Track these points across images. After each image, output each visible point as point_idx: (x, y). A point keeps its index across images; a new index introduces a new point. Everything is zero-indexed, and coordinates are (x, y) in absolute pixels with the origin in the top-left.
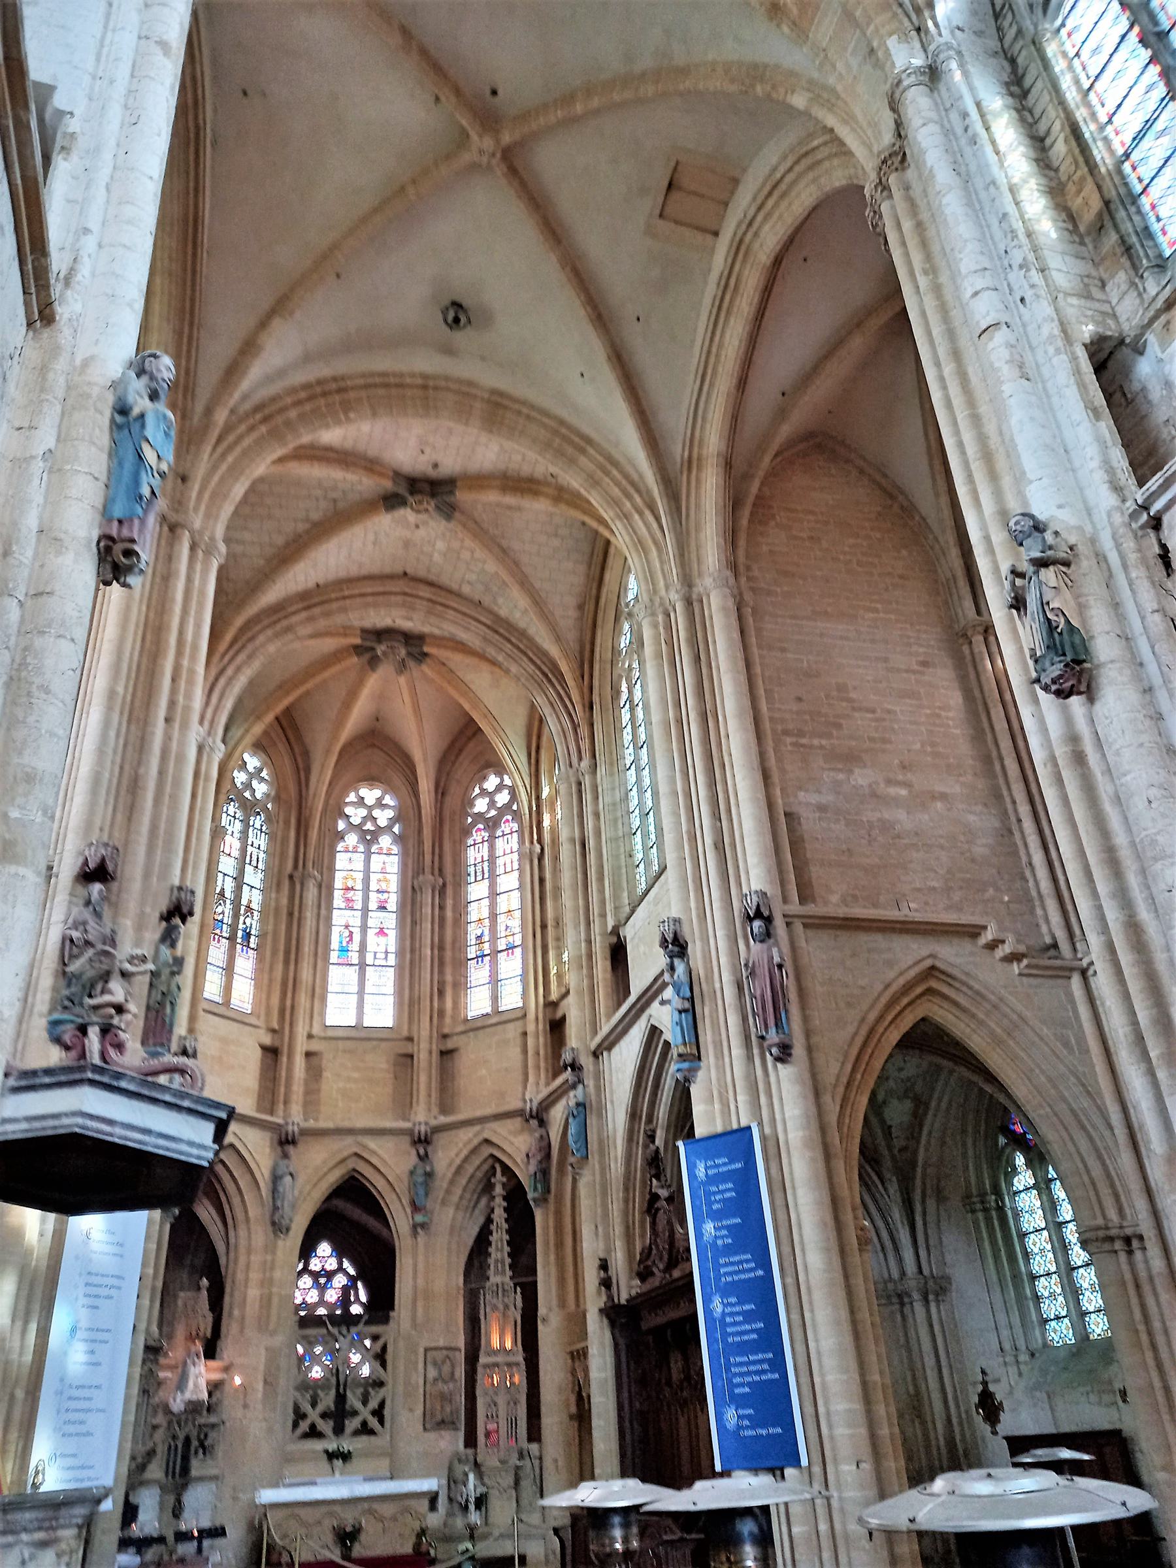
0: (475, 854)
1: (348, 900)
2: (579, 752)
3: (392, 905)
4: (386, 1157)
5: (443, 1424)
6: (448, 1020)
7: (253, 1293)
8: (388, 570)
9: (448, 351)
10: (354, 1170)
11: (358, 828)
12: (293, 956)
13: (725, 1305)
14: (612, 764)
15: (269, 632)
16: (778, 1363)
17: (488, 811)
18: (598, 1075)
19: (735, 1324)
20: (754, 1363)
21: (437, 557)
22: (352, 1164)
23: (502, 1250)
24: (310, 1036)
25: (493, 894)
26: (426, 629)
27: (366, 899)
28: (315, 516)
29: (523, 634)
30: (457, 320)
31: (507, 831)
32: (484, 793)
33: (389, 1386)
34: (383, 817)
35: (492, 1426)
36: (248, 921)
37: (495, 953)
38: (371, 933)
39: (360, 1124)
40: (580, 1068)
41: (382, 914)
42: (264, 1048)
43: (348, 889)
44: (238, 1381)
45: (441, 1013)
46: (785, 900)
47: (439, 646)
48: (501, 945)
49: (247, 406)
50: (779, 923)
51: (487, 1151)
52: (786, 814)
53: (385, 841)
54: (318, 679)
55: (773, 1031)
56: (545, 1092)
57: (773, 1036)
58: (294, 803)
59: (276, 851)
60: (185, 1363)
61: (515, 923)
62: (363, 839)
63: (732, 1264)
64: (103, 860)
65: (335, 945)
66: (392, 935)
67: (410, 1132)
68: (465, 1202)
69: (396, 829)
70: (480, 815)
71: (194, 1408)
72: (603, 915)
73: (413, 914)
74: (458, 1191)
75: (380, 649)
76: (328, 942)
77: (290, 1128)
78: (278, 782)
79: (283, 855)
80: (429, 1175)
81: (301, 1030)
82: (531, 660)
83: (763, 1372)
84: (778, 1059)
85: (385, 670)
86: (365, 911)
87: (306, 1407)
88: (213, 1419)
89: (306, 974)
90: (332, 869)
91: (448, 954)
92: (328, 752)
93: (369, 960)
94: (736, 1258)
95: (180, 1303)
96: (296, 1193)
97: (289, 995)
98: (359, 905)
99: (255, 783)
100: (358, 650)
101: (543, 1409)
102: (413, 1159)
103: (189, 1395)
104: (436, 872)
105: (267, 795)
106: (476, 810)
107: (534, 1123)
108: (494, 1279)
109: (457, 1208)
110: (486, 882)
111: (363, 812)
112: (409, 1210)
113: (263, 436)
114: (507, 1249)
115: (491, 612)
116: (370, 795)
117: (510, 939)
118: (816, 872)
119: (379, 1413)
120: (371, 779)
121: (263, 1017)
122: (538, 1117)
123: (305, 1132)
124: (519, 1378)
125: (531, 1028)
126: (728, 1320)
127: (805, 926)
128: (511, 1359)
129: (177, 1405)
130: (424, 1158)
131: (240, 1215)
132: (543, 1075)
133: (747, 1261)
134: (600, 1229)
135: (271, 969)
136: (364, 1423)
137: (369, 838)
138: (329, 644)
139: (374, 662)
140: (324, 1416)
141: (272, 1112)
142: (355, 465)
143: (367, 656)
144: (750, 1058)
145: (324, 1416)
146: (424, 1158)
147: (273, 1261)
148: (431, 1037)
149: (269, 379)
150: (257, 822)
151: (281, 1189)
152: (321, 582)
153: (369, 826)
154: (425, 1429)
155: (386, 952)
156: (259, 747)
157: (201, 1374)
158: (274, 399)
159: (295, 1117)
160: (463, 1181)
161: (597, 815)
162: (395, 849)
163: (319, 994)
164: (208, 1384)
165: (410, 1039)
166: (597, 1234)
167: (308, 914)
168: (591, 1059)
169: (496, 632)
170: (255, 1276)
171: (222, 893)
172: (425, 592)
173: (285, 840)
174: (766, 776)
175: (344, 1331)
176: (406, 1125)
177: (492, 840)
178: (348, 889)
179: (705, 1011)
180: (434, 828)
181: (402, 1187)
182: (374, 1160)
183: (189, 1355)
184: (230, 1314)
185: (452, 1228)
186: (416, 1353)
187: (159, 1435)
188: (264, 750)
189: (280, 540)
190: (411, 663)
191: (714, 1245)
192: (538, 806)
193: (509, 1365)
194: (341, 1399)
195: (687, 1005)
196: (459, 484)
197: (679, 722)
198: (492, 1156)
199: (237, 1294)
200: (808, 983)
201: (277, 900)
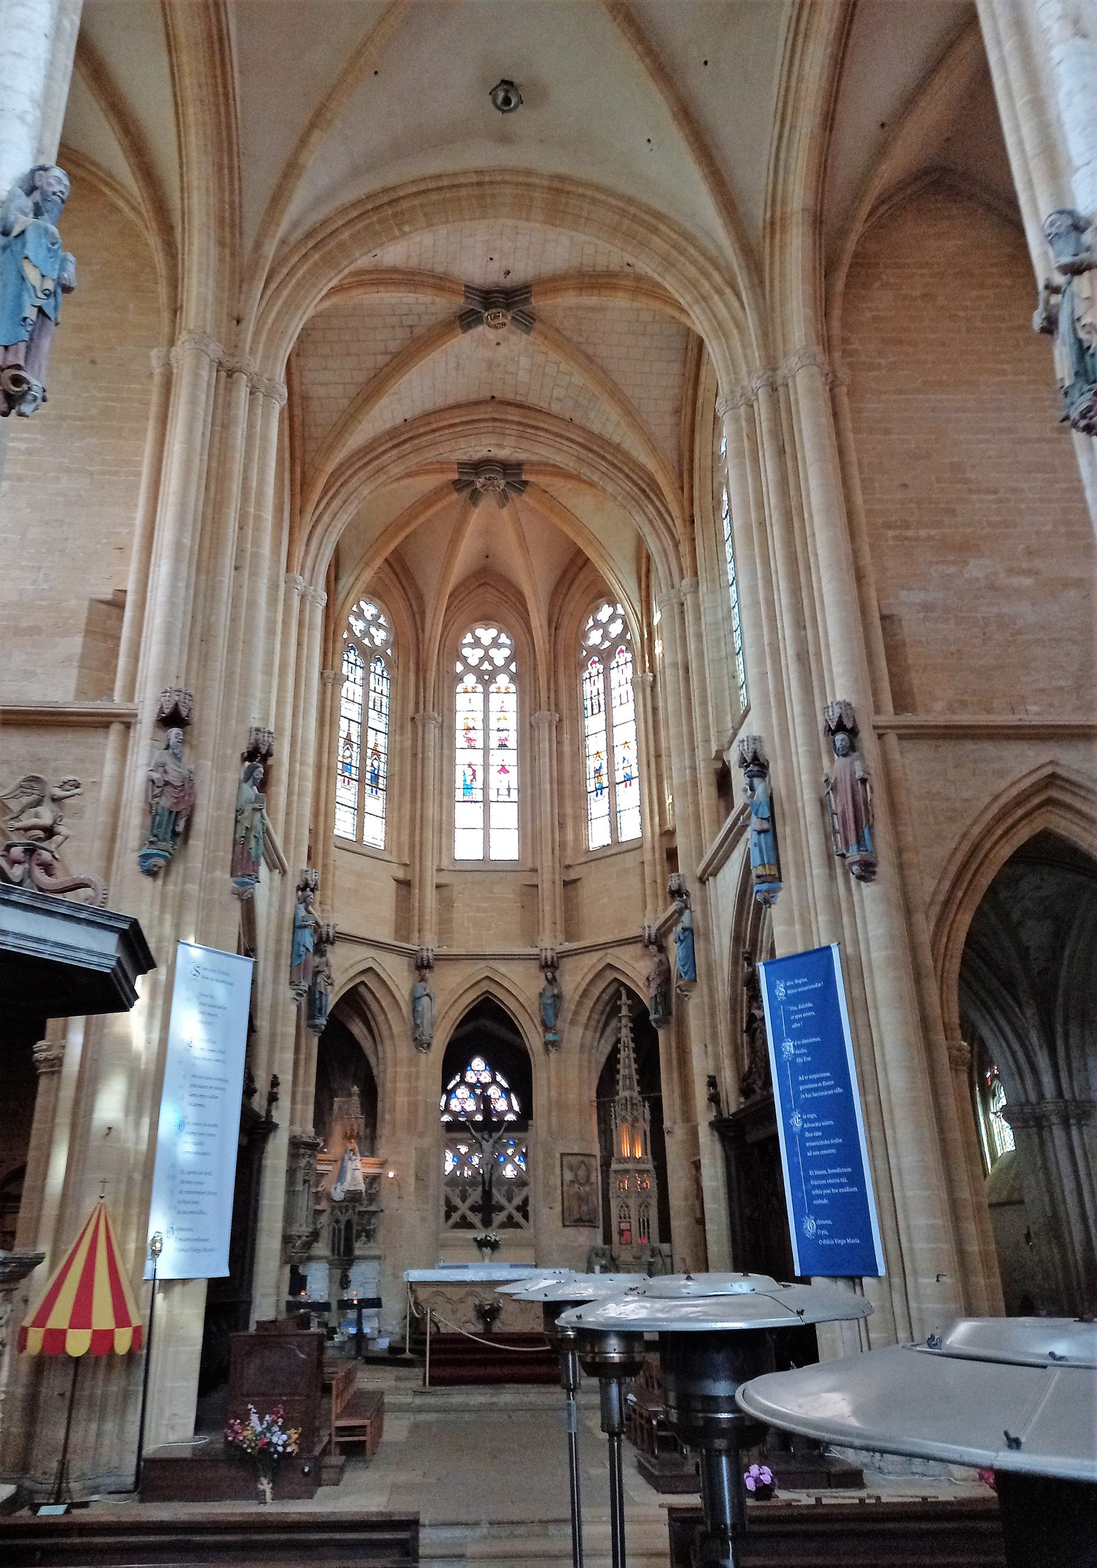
0: (592, 687)
1: (469, 740)
2: (681, 570)
3: (512, 743)
4: (516, 980)
5: (580, 1222)
6: (569, 852)
7: (401, 1100)
8: (473, 397)
9: (505, 139)
10: (487, 992)
11: (476, 670)
12: (419, 795)
13: (804, 1121)
14: (713, 581)
15: (362, 474)
16: (857, 1178)
17: (602, 643)
18: (704, 902)
19: (813, 1139)
20: (833, 1176)
21: (523, 376)
22: (485, 986)
23: (629, 1067)
24: (439, 870)
25: (609, 727)
26: (522, 456)
27: (486, 738)
28: (393, 346)
29: (617, 448)
30: (507, 101)
31: (622, 661)
32: (597, 625)
33: (531, 1186)
34: (500, 656)
35: (624, 1226)
36: (376, 763)
37: (613, 785)
38: (493, 771)
39: (489, 950)
40: (687, 894)
41: (503, 752)
42: (397, 881)
43: (469, 729)
45: (563, 845)
46: (878, 710)
47: (537, 473)
48: (619, 777)
49: (299, 234)
50: (867, 738)
51: (611, 975)
52: (883, 618)
53: (503, 680)
54: (422, 519)
55: (854, 848)
56: (662, 918)
57: (854, 855)
58: (412, 647)
59: (397, 696)
60: (343, 1160)
61: (631, 755)
62: (480, 679)
63: (813, 1081)
64: (176, 705)
65: (459, 783)
66: (514, 772)
67: (536, 958)
68: (593, 1023)
69: (513, 667)
70: (594, 650)
71: (353, 1197)
72: (707, 741)
73: (532, 749)
74: (585, 1013)
75: (479, 482)
76: (452, 781)
77: (425, 954)
78: (395, 629)
79: (404, 699)
80: (558, 997)
81: (430, 865)
82: (627, 476)
83: (842, 1185)
84: (860, 878)
85: (487, 503)
86: (486, 750)
87: (457, 1201)
88: (372, 1208)
89: (431, 810)
90: (452, 711)
91: (568, 787)
92: (440, 593)
93: (493, 796)
94: (816, 1076)
95: (336, 1107)
96: (435, 1012)
97: (418, 831)
98: (480, 744)
99: (373, 630)
100: (458, 485)
101: (672, 1213)
102: (543, 983)
103: (347, 1186)
104: (553, 706)
105: (385, 642)
106: (590, 643)
107: (653, 949)
108: (624, 1094)
109: (586, 1027)
110: (603, 714)
111: (480, 653)
112: (540, 1029)
113: (316, 264)
114: (634, 1066)
115: (582, 428)
116: (486, 635)
117: (628, 770)
118: (917, 680)
119: (523, 1209)
120: (486, 620)
121: (395, 853)
122: (657, 943)
123: (438, 958)
124: (650, 1183)
125: (648, 856)
126: (807, 1135)
127: (900, 737)
128: (642, 1166)
129: (338, 1195)
130: (552, 981)
131: (385, 1033)
132: (660, 903)
133: (827, 1079)
134: (710, 1049)
135: (400, 808)
136: (510, 1217)
137: (486, 679)
138: (428, 483)
139: (475, 497)
140: (473, 1209)
141: (407, 939)
142: (423, 284)
143: (466, 493)
144: (832, 877)
145: (473, 1209)
146: (552, 981)
147: (417, 1073)
148: (554, 868)
149: (317, 202)
150: (379, 668)
151: (420, 1009)
152: (408, 416)
153: (486, 666)
154: (564, 1226)
155: (509, 789)
156: (374, 594)
158: (324, 223)
159: (430, 944)
160: (590, 1003)
161: (699, 636)
162: (513, 688)
163: (446, 829)
164: (366, 1177)
165: (534, 870)
166: (706, 1053)
167: (431, 755)
168: (698, 885)
169: (590, 450)
170: (402, 1085)
171: (348, 739)
172: (514, 415)
173: (405, 684)
174: (860, 577)
175: (486, 1136)
176: (536, 951)
177: (606, 673)
178: (469, 729)
179: (785, 831)
180: (548, 664)
181: (533, 1007)
182: (505, 984)
183: (345, 1152)
184: (384, 1120)
185: (582, 1046)
186: (553, 1157)
187: (324, 1219)
188: (380, 597)
189: (361, 377)
190: (512, 494)
191: (793, 1062)
192: (650, 634)
193: (641, 1172)
194: (487, 1195)
195: (766, 825)
196: (534, 289)
197: (762, 524)
198: (616, 979)
199: (387, 1100)
200: (901, 797)
201: (402, 742)
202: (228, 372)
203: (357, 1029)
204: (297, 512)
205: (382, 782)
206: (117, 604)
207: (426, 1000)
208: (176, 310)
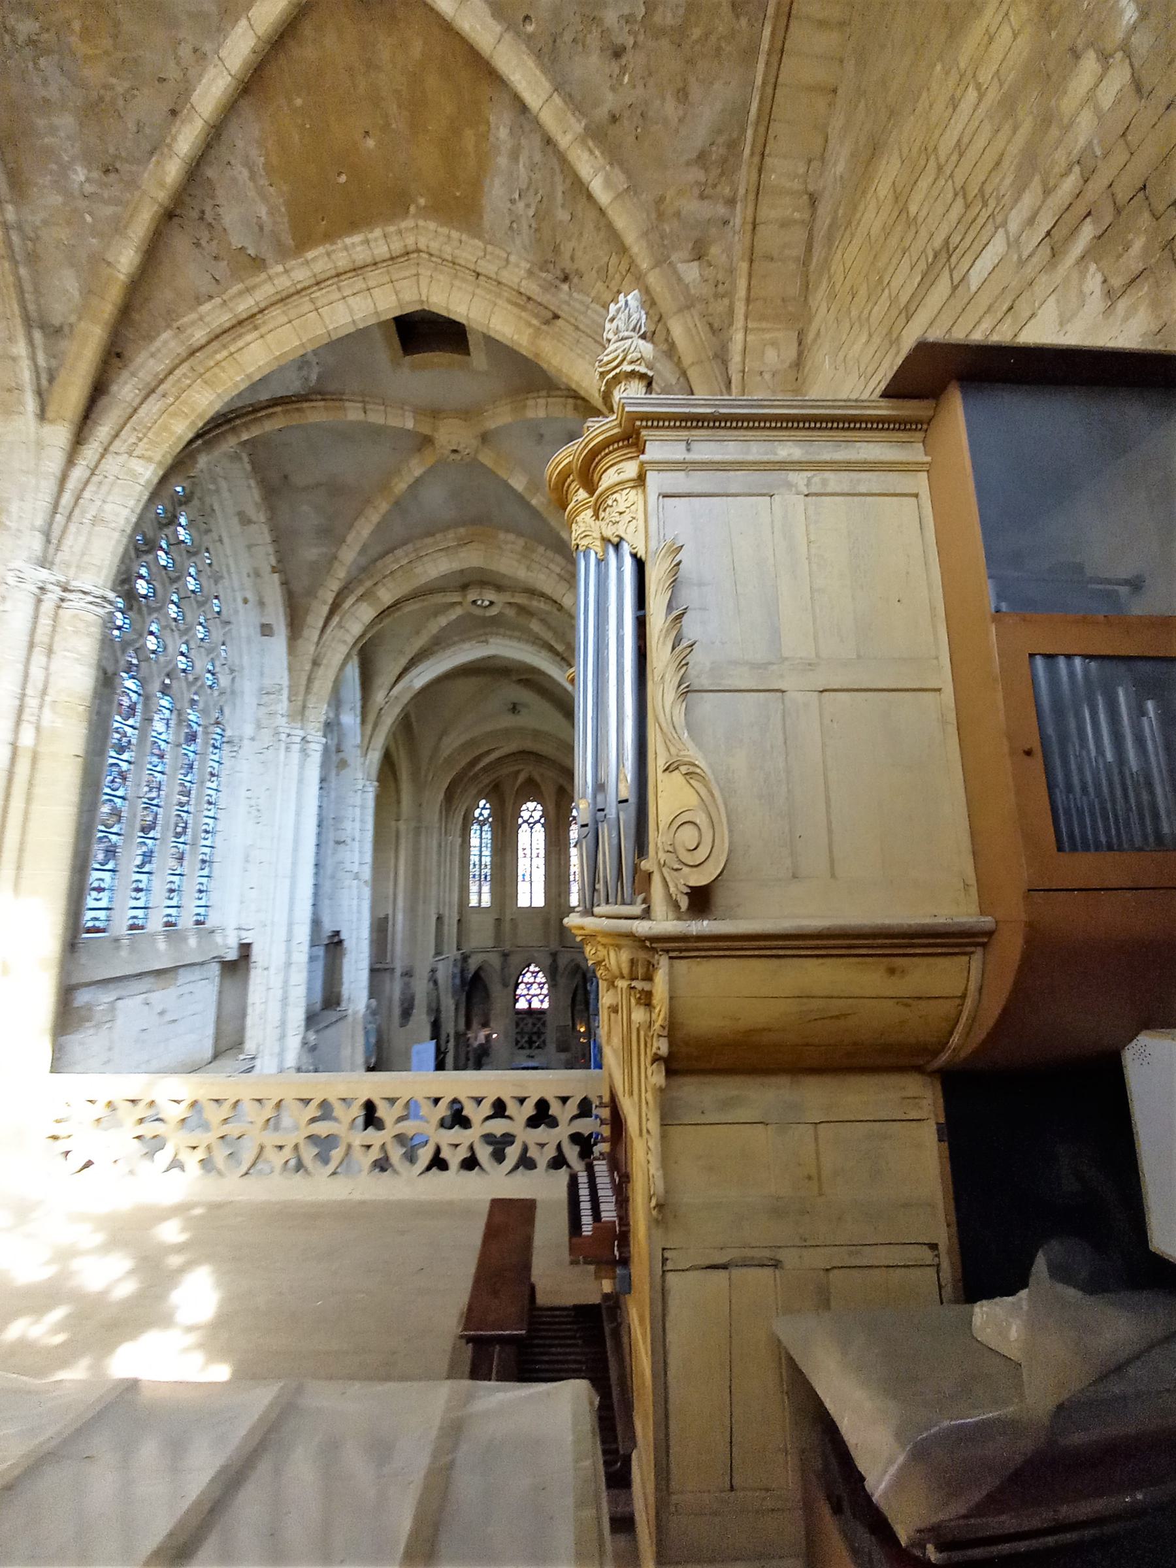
3: (542, 854)
34: (537, 815)
43: (524, 849)
44: (495, 1036)
69: (542, 821)
71: (481, 1045)
81: (508, 912)
105: (489, 816)
116: (531, 805)
119: (544, 1042)
129: (476, 1044)
130: (554, 961)
145: (526, 1042)
146: (554, 961)
157: (482, 1034)
159: (507, 947)
178: (524, 849)
202: (417, 831)
203: (483, 974)
204: (448, 810)
206: (386, 918)
208: (399, 802)
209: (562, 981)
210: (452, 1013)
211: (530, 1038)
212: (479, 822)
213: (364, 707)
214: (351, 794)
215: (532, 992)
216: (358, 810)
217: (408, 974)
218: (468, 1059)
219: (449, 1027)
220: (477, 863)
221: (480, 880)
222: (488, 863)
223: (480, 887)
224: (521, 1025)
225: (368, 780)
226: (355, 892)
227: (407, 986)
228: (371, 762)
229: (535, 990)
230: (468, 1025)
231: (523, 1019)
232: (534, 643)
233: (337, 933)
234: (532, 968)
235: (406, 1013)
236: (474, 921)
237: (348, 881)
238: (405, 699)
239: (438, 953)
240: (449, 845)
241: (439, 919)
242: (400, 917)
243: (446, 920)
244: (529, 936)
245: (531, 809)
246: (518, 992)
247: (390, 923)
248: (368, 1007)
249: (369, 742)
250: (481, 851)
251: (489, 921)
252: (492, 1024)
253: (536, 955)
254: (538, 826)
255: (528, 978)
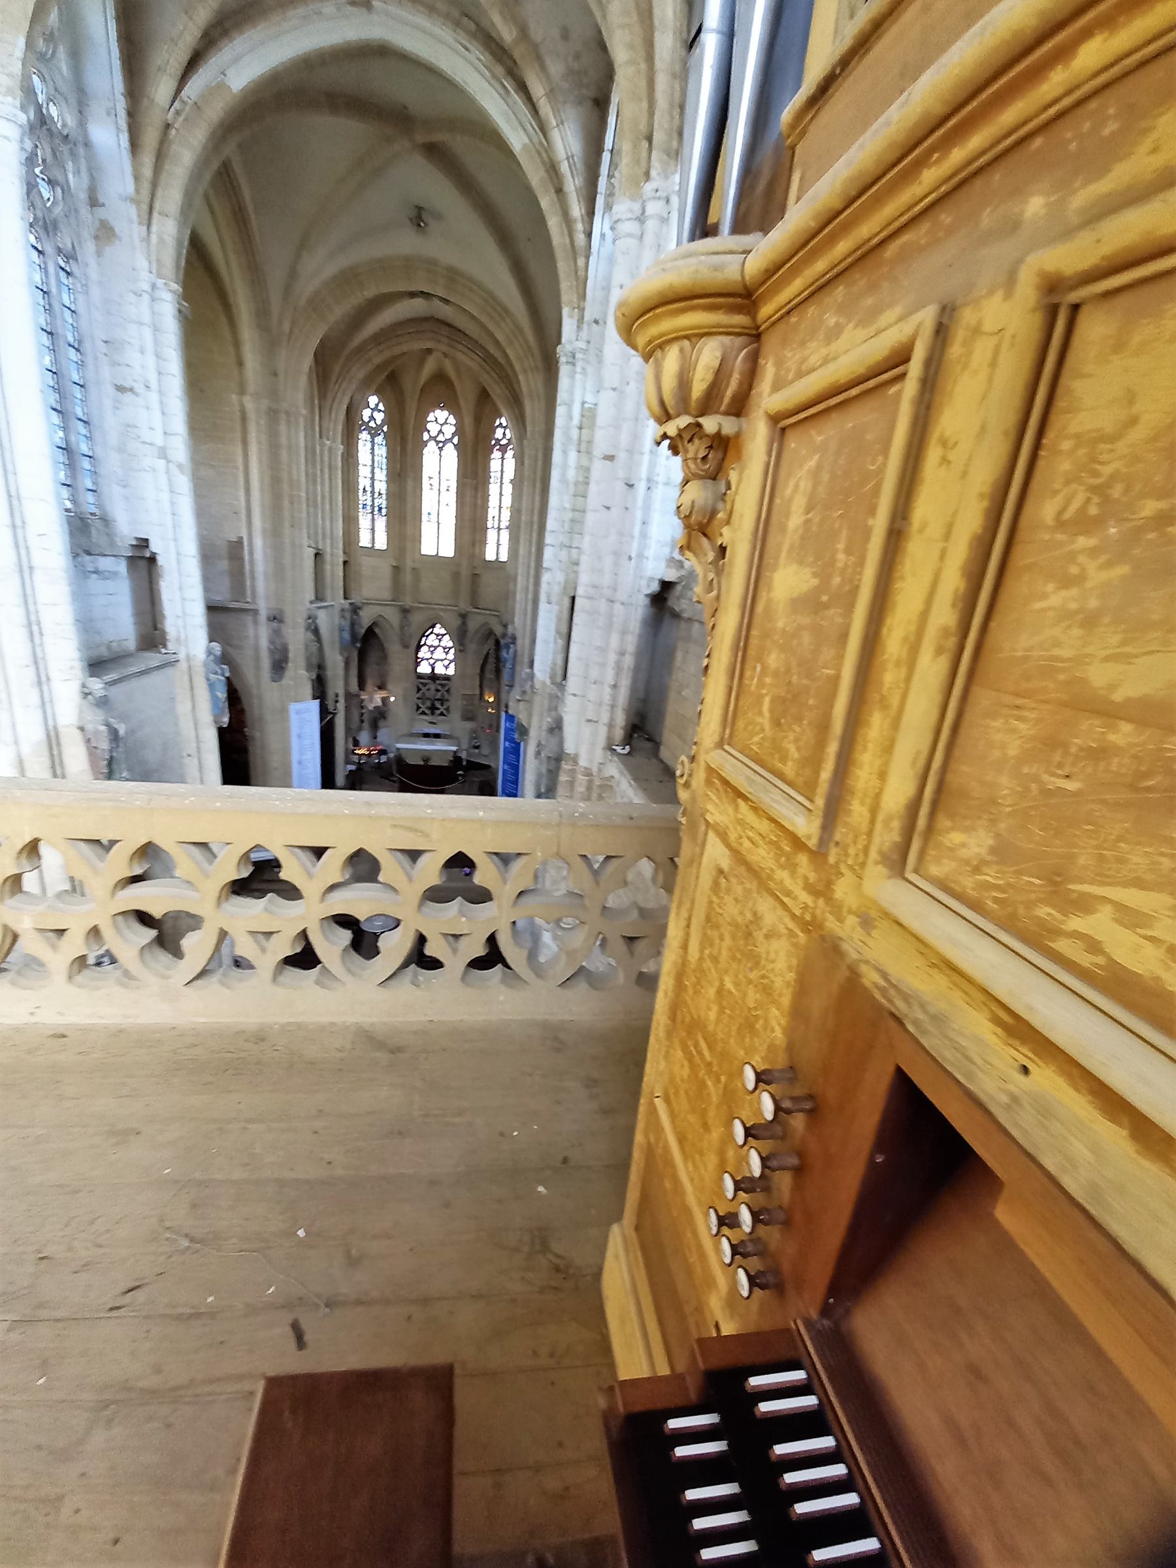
43: (430, 478)
44: (392, 699)
59: (390, 457)
119: (447, 709)
129: (371, 707)
130: (464, 623)
146: (464, 623)
156: (377, 392)
159: (408, 601)
202: (273, 415)
203: (377, 630)
205: (384, 511)
206: (240, 542)
207: (406, 628)
208: (240, 364)
209: (472, 647)
210: (341, 671)
211: (433, 705)
212: (369, 429)
213: (132, 114)
214: (132, 298)
215: (435, 656)
216: (147, 333)
217: (276, 618)
218: (362, 721)
219: (337, 686)
220: (369, 489)
221: (372, 513)
222: (383, 492)
223: (373, 520)
224: (424, 689)
225: (159, 276)
226: (163, 479)
227: (277, 633)
228: (161, 241)
229: (439, 654)
230: (362, 685)
231: (425, 685)
232: (457, 24)
233: (144, 543)
234: (438, 629)
235: (279, 665)
236: (366, 563)
237: (150, 460)
238: (215, 112)
239: (319, 597)
240: (326, 453)
241: (318, 555)
242: (258, 542)
243: (328, 558)
244: (434, 590)
245: (441, 421)
246: (420, 655)
247: (246, 548)
248: (209, 652)
249: (153, 195)
250: (373, 473)
251: (384, 569)
252: (390, 686)
253: (442, 614)
254: (450, 446)
255: (432, 640)
